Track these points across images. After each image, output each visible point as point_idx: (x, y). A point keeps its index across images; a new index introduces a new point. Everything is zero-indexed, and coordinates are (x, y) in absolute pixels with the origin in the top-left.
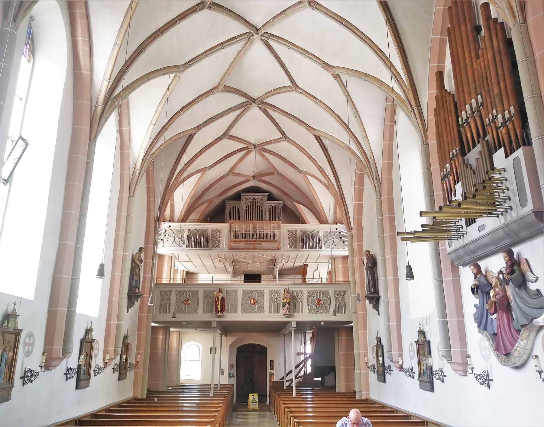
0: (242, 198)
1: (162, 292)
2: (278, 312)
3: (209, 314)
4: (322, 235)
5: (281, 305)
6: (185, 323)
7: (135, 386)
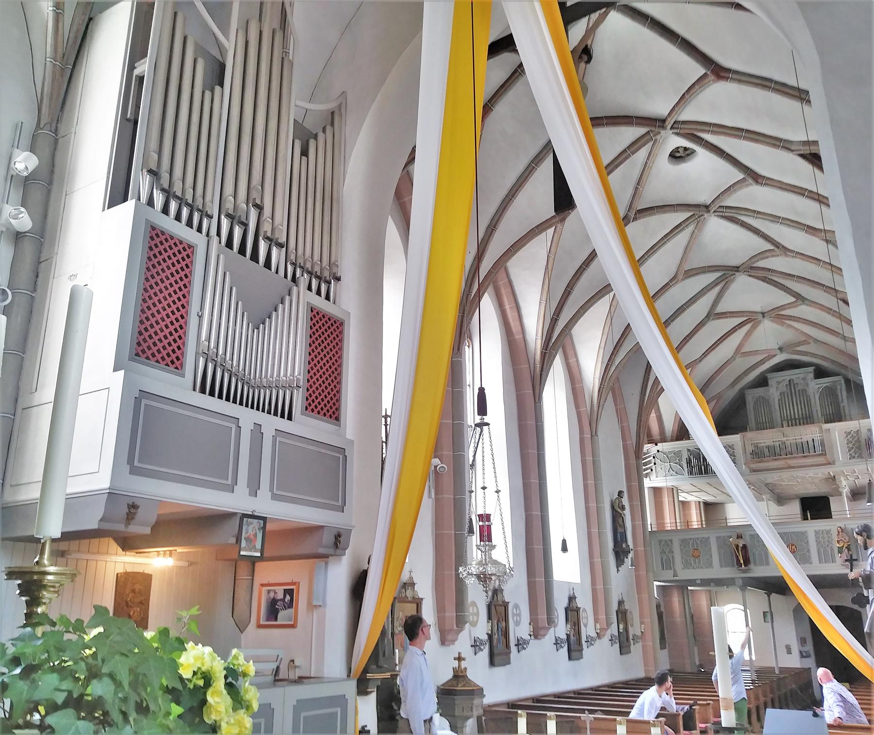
0: (770, 382)
1: (660, 541)
2: (834, 561)
6: (699, 582)
7: (646, 663)
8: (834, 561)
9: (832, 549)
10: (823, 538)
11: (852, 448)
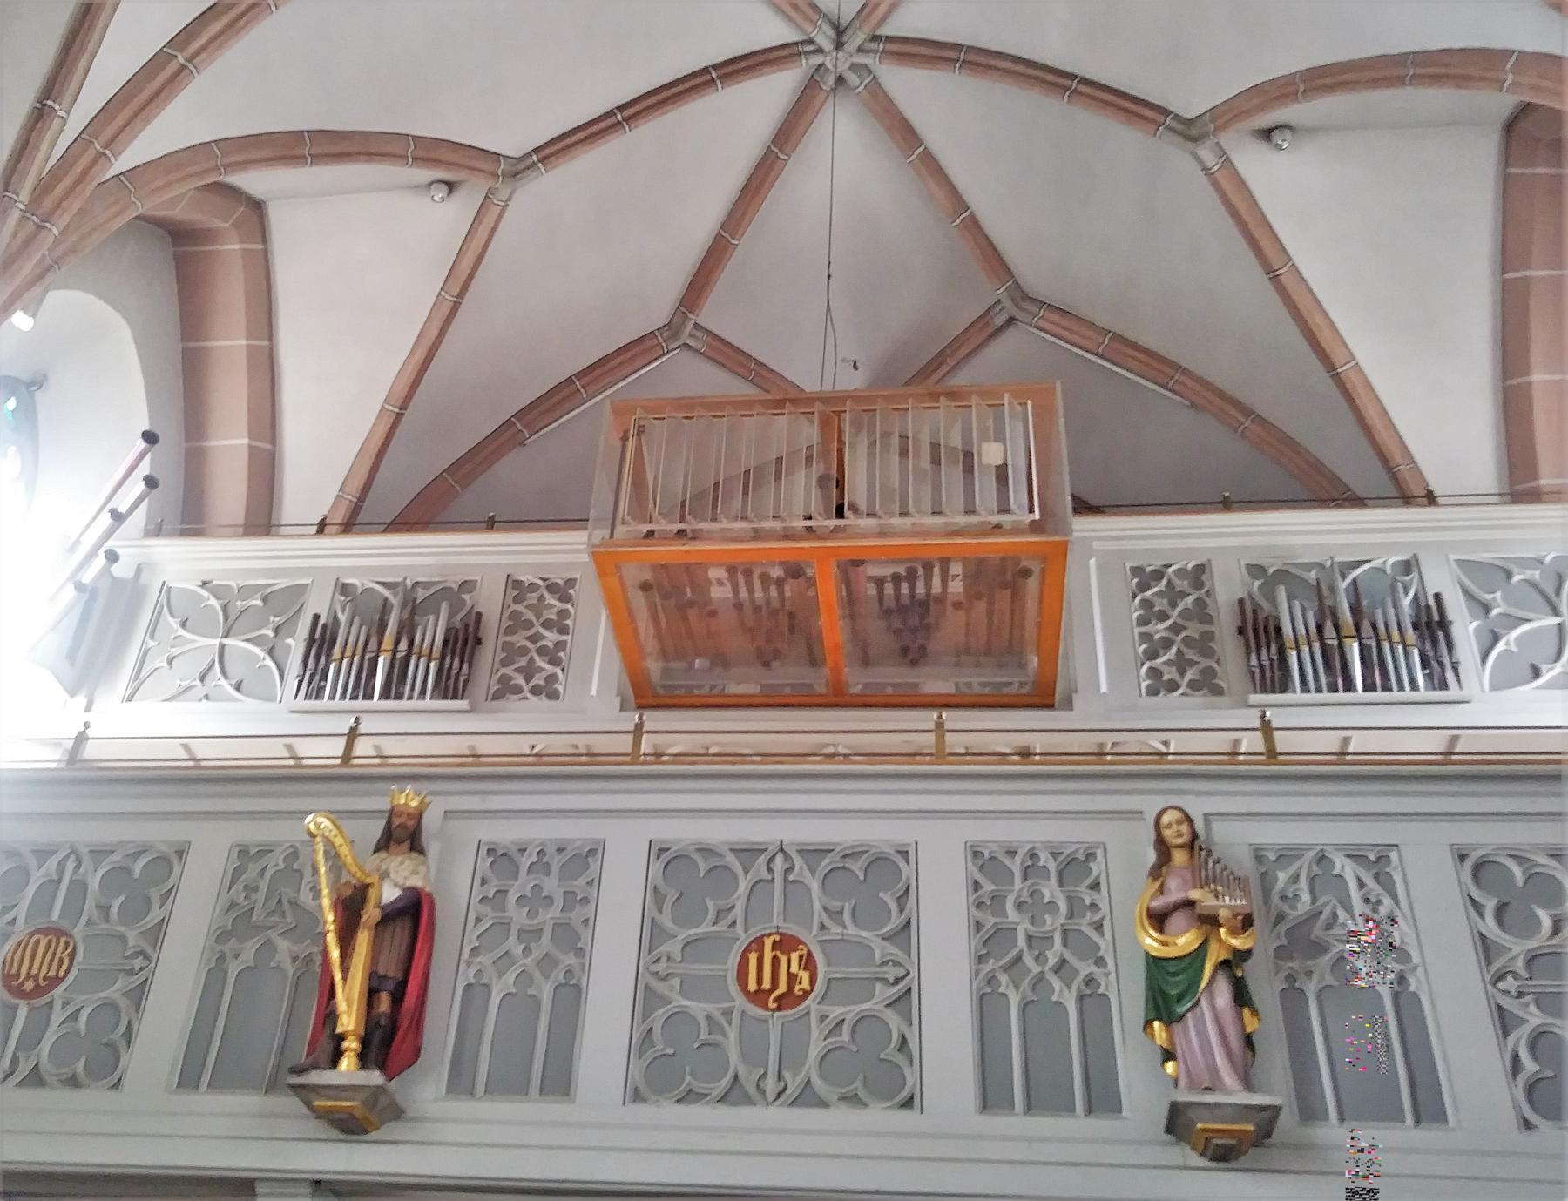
3: (250, 1101)
5: (1127, 996)
9: (1092, 998)
10: (1032, 906)
11: (1167, 643)
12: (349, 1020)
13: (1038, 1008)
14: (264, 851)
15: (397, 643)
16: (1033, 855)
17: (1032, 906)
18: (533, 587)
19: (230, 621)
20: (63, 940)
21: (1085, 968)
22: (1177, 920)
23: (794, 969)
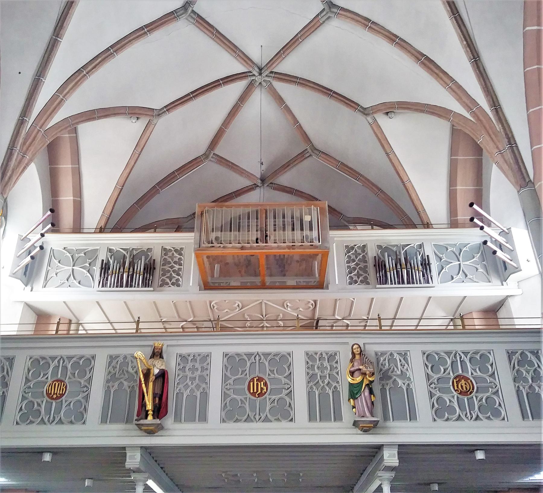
2: (338, 417)
4: (429, 251)
5: (345, 392)
8: (338, 417)
9: (336, 392)
10: (322, 368)
11: (355, 269)
12: (149, 406)
13: (323, 396)
14: (117, 357)
15: (129, 269)
16: (321, 354)
17: (322, 368)
18: (170, 250)
19: (75, 260)
20: (62, 383)
21: (334, 384)
22: (356, 373)
23: (262, 386)
